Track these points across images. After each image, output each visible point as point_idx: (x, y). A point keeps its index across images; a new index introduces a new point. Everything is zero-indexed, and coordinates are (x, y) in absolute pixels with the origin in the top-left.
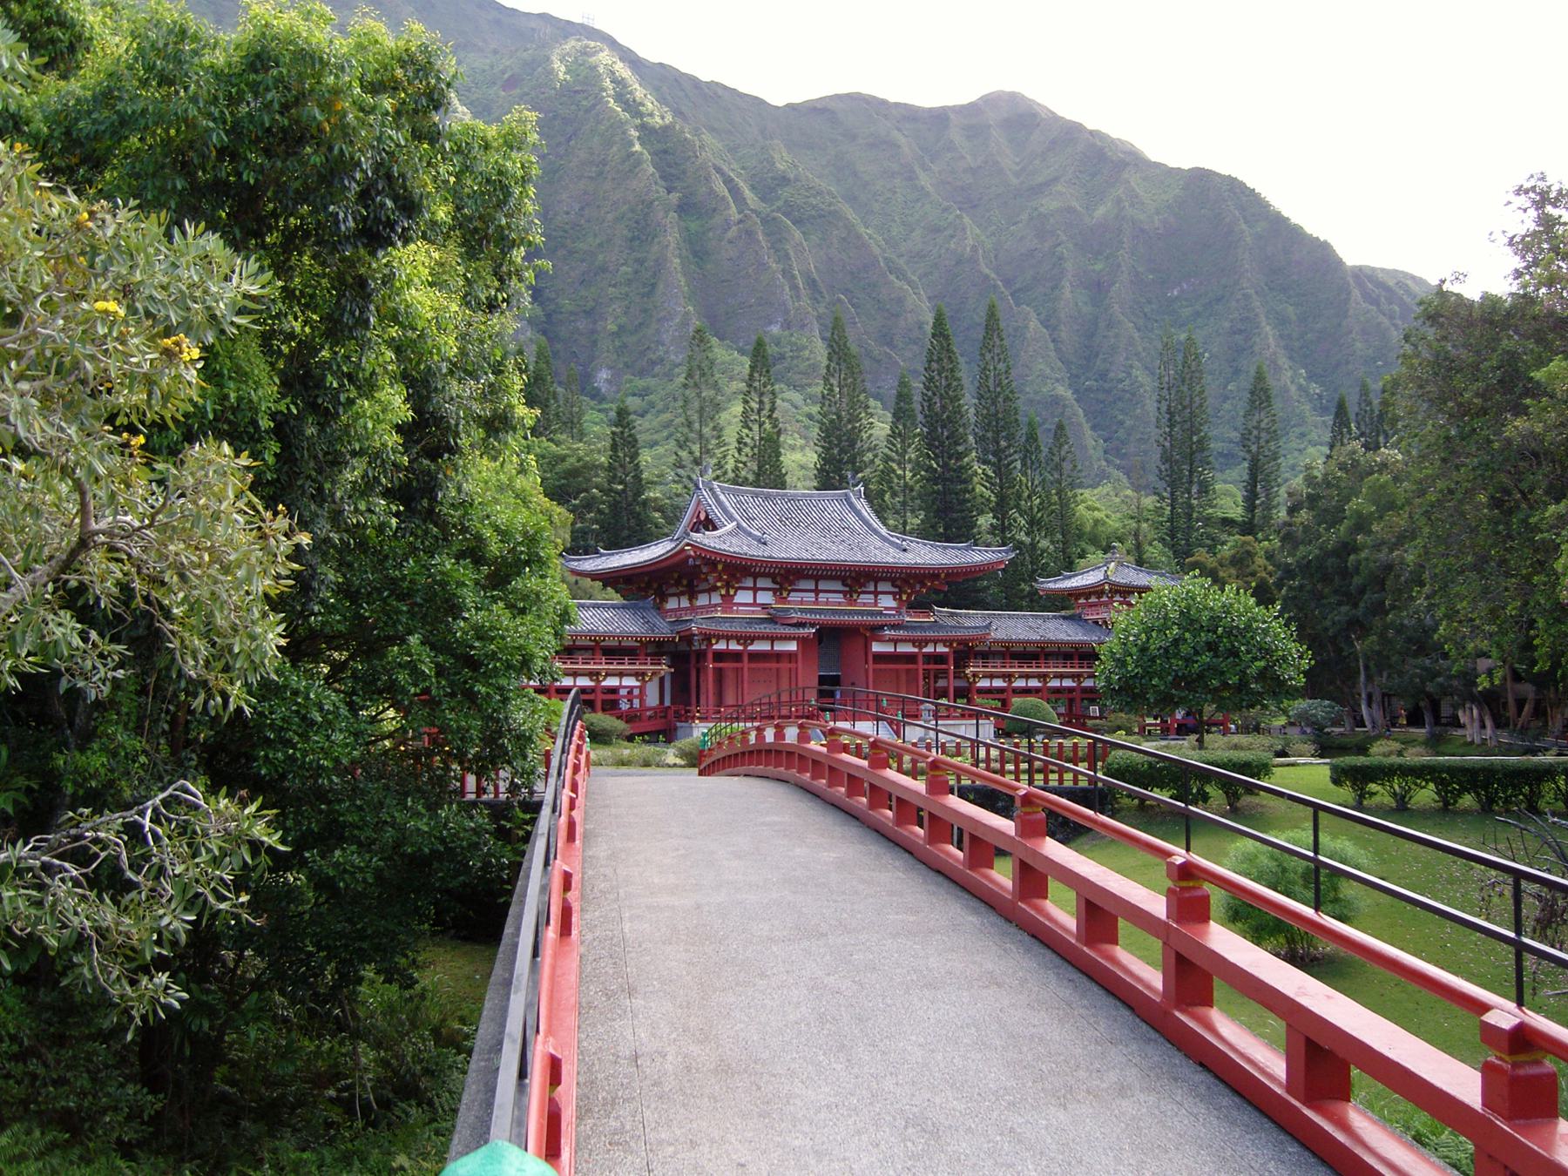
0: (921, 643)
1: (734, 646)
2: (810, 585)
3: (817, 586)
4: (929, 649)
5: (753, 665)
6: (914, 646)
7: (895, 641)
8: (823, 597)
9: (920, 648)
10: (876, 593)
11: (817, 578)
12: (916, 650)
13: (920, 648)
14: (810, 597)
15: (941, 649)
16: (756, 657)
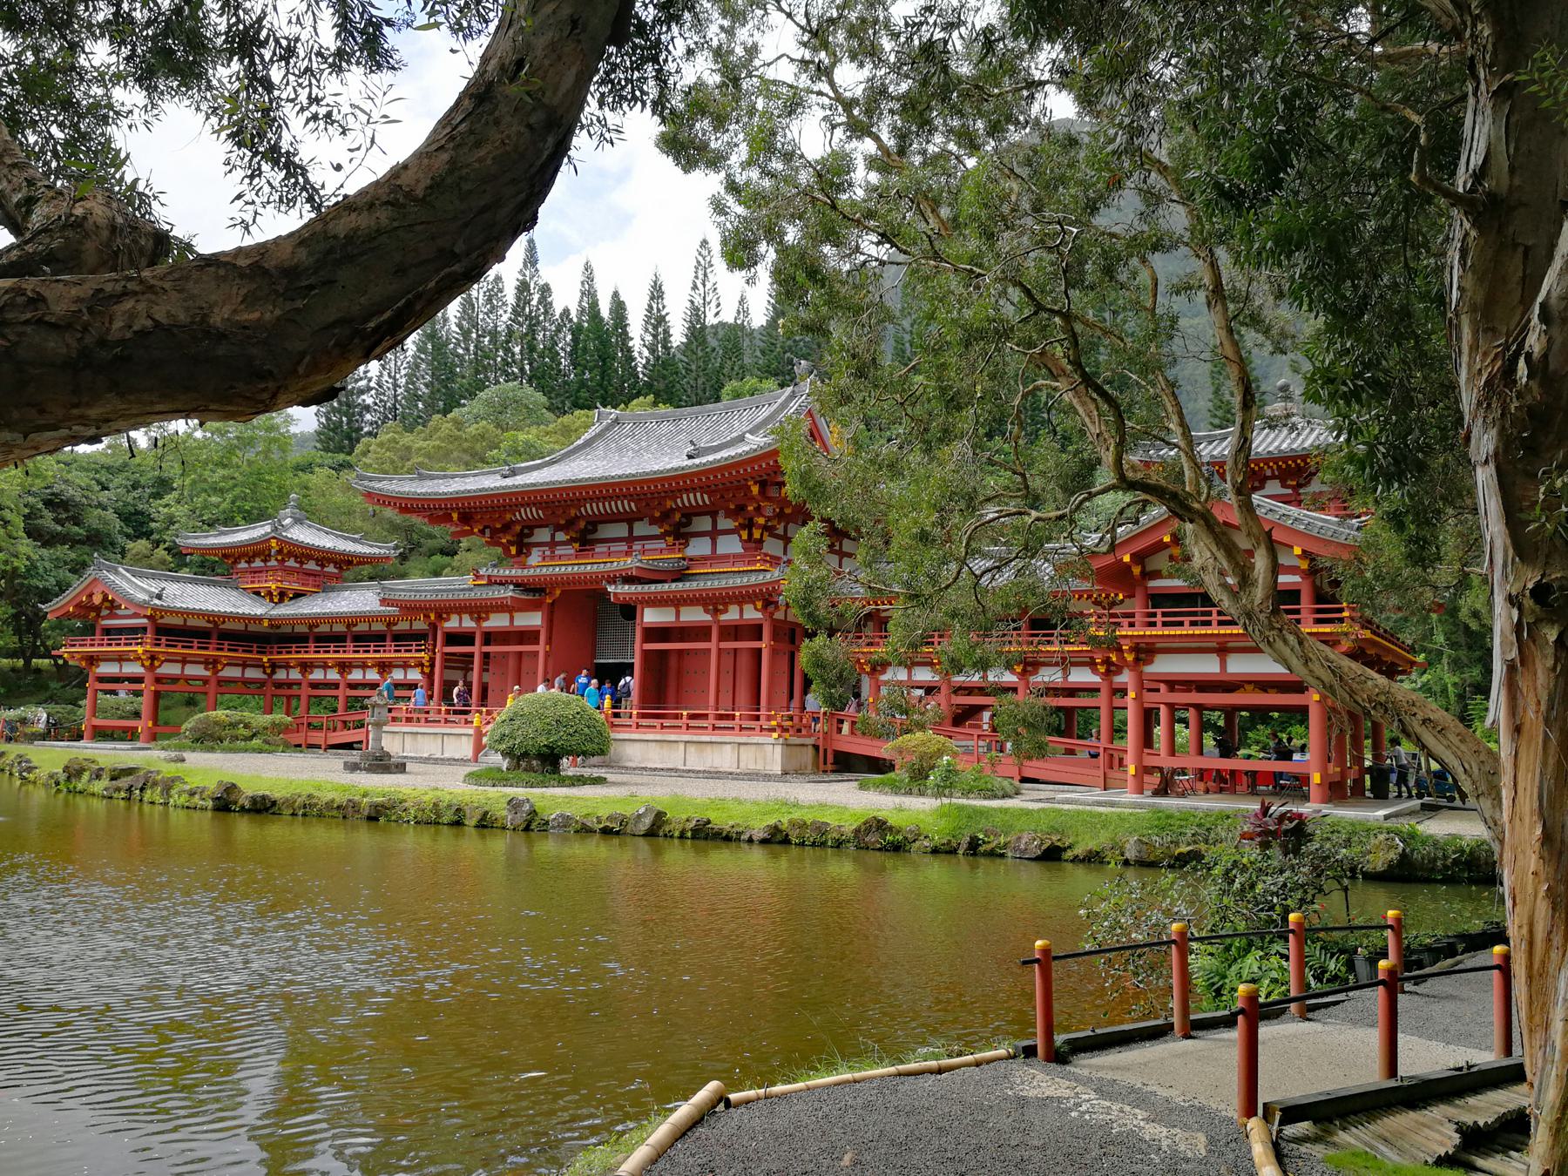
0: (715, 602)
1: (468, 623)
2: (621, 530)
3: (631, 530)
4: (731, 615)
5: (486, 649)
6: (706, 611)
7: (677, 602)
8: (637, 546)
9: (716, 612)
10: (714, 534)
11: (629, 519)
12: (708, 618)
13: (716, 612)
14: (623, 547)
15: (752, 614)
16: (489, 637)
